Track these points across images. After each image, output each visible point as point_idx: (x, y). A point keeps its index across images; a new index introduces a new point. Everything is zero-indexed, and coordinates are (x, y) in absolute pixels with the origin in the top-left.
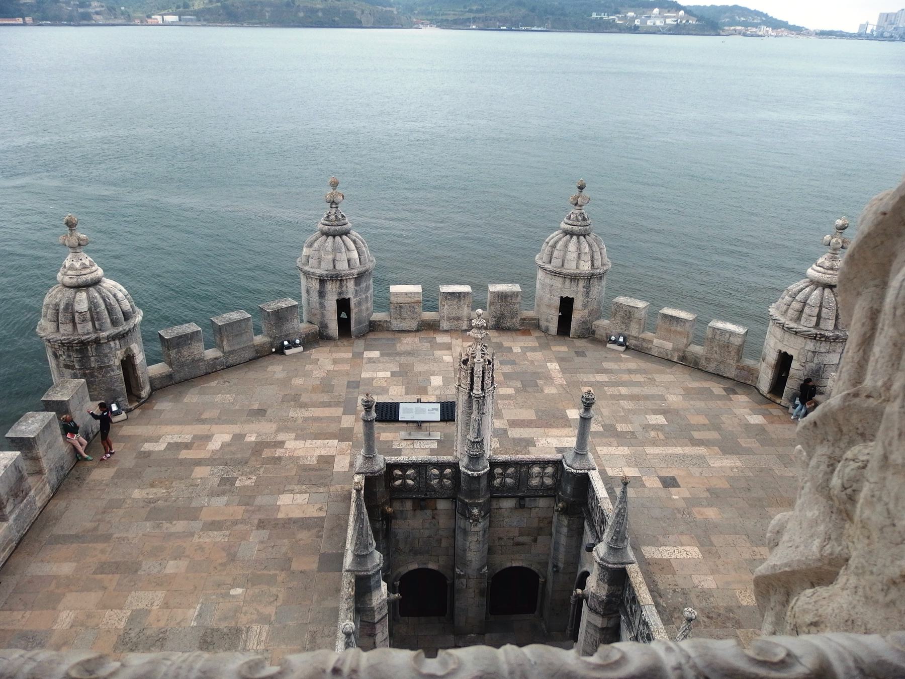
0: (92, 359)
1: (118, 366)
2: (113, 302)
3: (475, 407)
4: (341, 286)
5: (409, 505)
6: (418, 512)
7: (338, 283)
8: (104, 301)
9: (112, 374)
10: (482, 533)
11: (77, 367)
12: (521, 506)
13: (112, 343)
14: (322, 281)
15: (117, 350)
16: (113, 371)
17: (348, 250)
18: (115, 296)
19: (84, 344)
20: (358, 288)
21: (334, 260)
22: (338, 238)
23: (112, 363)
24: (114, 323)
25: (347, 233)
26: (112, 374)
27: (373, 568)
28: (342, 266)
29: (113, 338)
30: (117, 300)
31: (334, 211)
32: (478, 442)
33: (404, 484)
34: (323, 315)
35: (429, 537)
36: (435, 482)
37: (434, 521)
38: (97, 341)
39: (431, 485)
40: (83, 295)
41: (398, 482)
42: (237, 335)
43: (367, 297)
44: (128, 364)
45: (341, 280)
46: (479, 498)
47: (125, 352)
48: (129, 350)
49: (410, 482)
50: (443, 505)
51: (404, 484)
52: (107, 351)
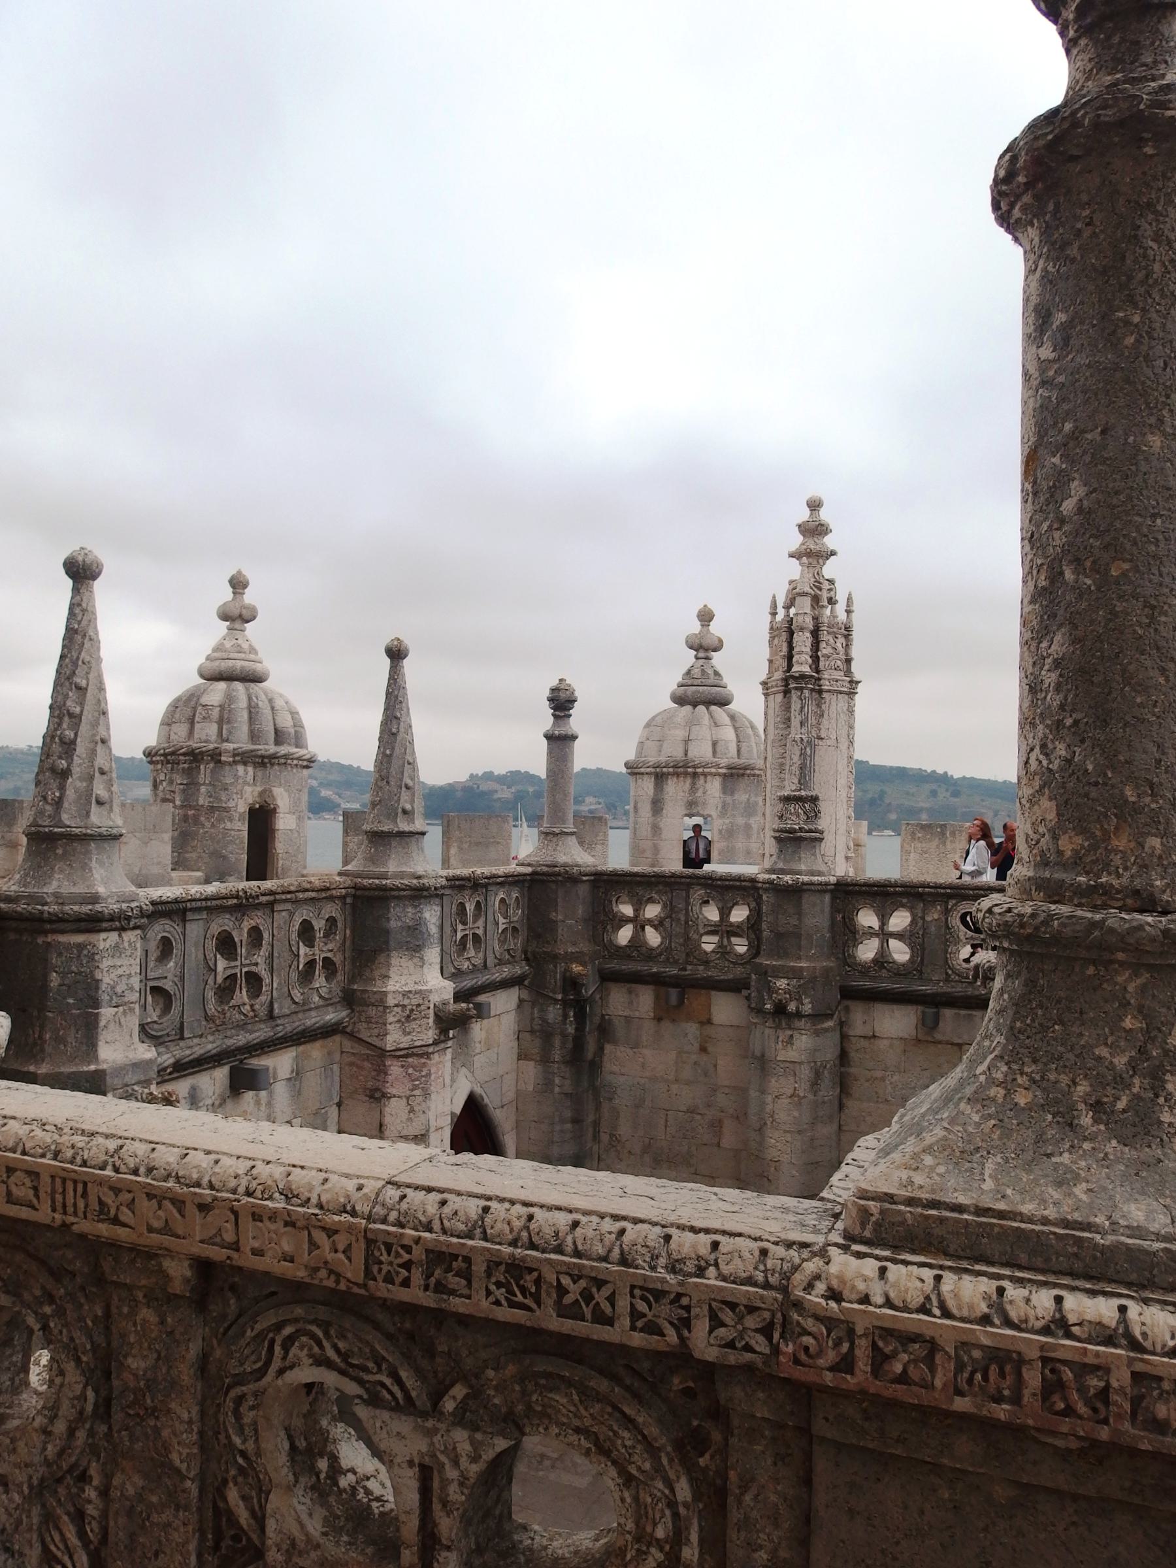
0: (203, 789)
1: (241, 815)
2: (263, 704)
3: (796, 705)
4: (693, 789)
5: (645, 999)
6: (666, 1025)
7: (689, 781)
8: (250, 699)
9: (228, 825)
10: (805, 1072)
11: (178, 803)
12: (930, 1025)
13: (241, 769)
14: (660, 778)
15: (248, 784)
16: (231, 819)
17: (716, 725)
18: (271, 701)
19: (195, 756)
20: (729, 799)
21: (687, 741)
22: (701, 708)
23: (231, 804)
24: (254, 736)
25: (723, 702)
26: (228, 825)
27: (402, 875)
28: (701, 751)
29: (244, 758)
30: (273, 708)
31: (701, 662)
32: (799, 799)
33: (637, 941)
34: (656, 850)
35: (692, 1111)
36: (709, 944)
37: (705, 1058)
38: (215, 756)
39: (698, 946)
40: (222, 685)
41: (624, 935)
42: (478, 844)
43: (748, 827)
44: (261, 820)
45: (695, 775)
46: (799, 958)
47: (261, 794)
48: (266, 793)
49: (653, 938)
50: (726, 1010)
51: (637, 941)
52: (229, 780)
